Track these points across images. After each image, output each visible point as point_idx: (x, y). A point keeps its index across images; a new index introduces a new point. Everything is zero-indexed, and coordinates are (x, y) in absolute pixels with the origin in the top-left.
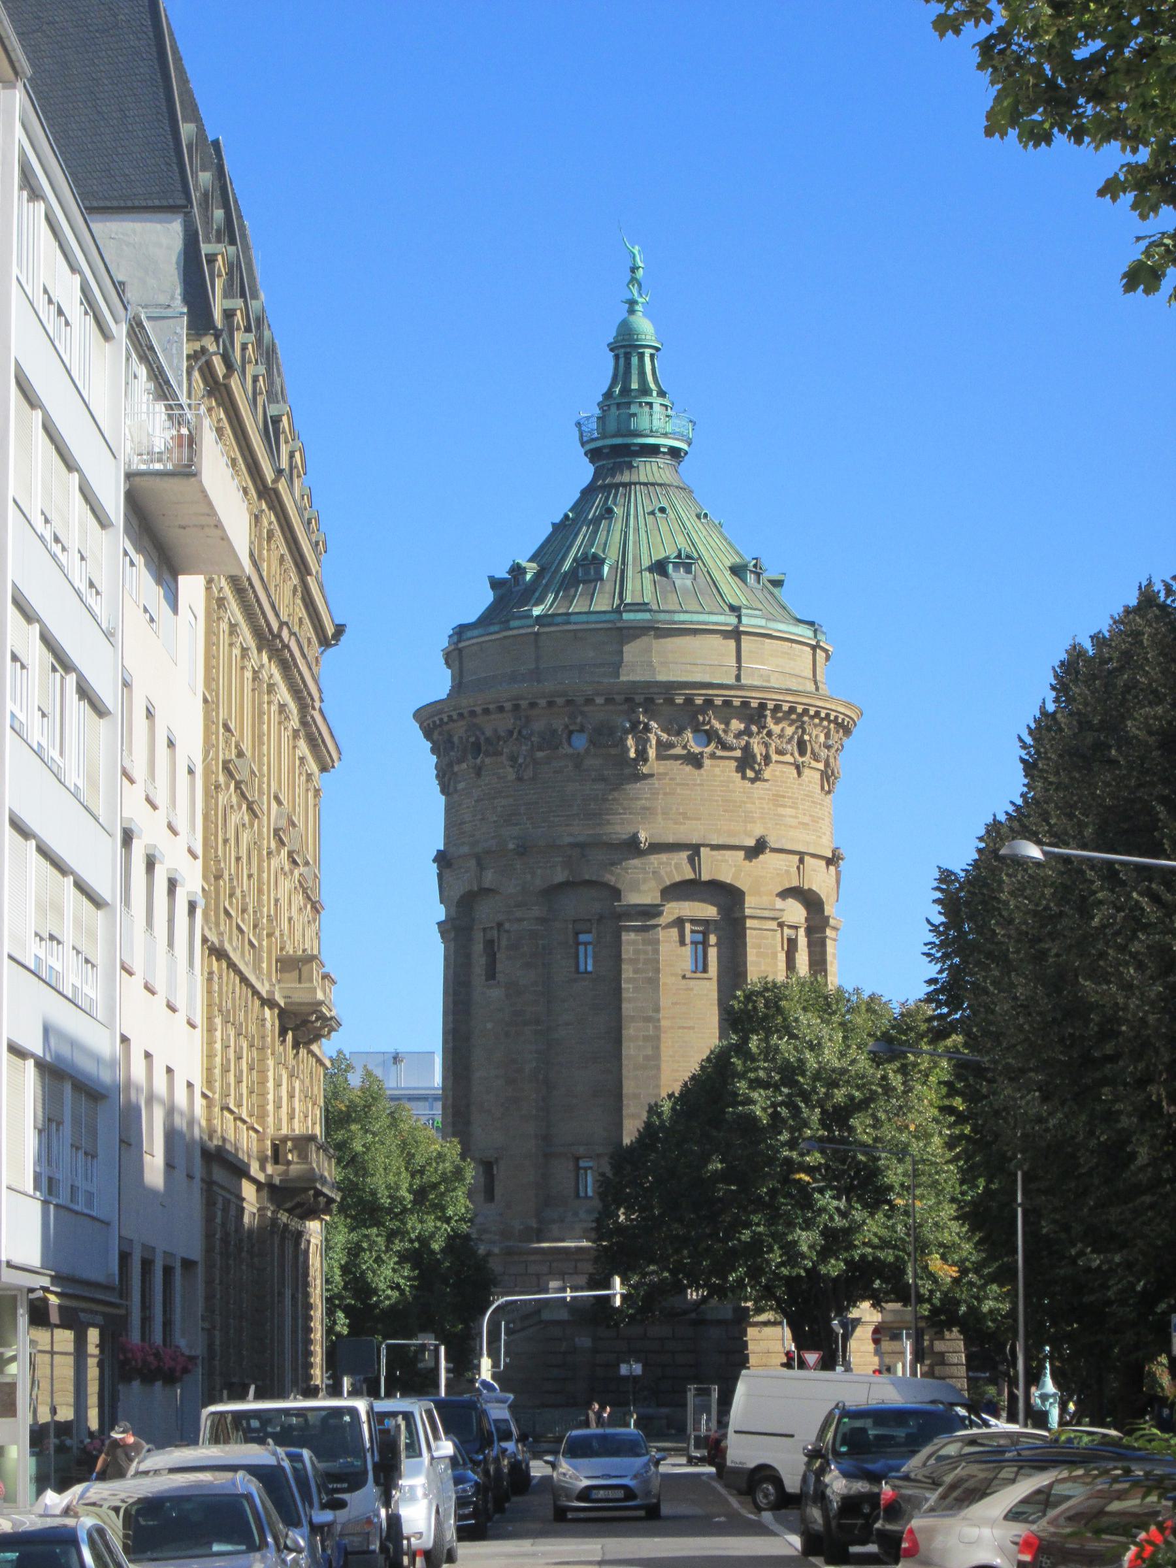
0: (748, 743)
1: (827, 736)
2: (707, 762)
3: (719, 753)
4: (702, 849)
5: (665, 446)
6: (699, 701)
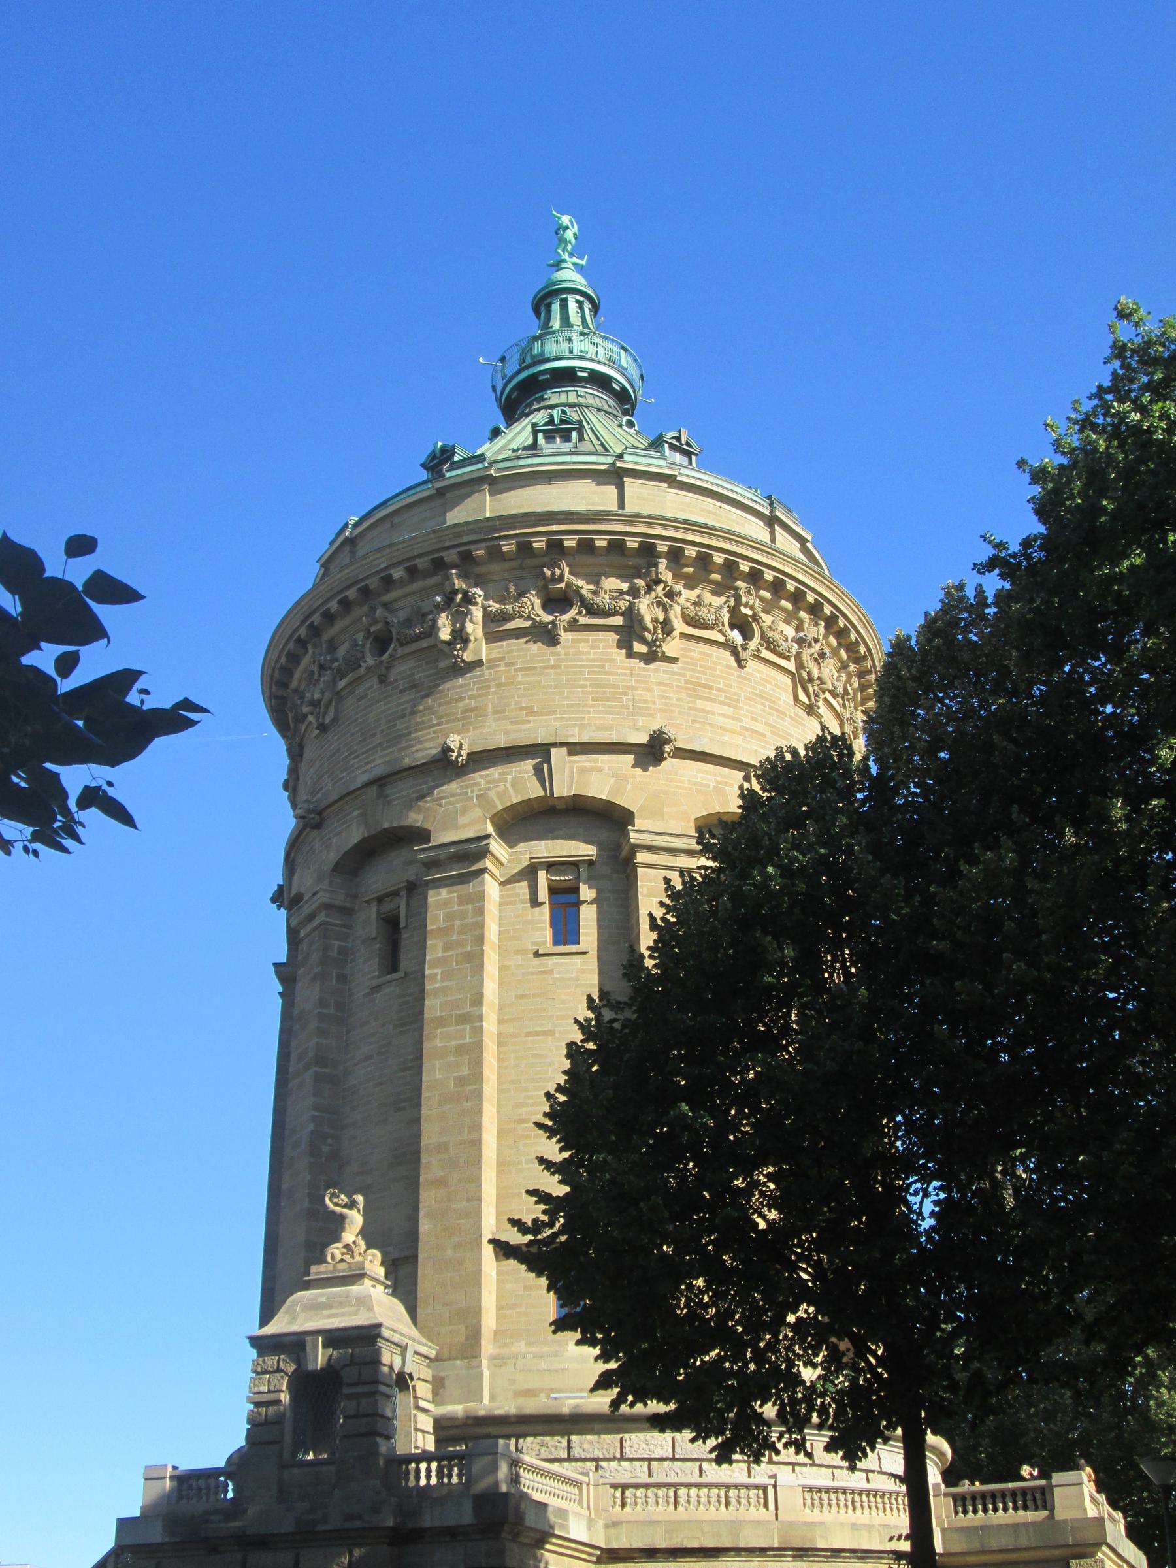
0: (632, 605)
1: (799, 629)
2: (565, 637)
3: (582, 620)
4: (553, 751)
5: (583, 369)
6: (539, 544)
